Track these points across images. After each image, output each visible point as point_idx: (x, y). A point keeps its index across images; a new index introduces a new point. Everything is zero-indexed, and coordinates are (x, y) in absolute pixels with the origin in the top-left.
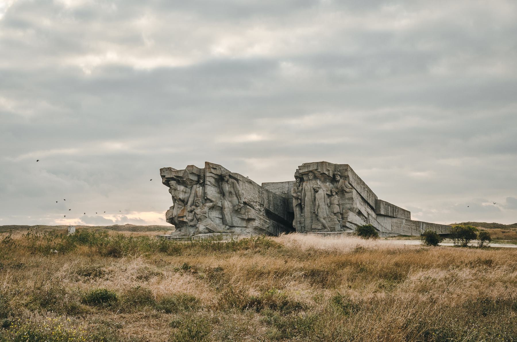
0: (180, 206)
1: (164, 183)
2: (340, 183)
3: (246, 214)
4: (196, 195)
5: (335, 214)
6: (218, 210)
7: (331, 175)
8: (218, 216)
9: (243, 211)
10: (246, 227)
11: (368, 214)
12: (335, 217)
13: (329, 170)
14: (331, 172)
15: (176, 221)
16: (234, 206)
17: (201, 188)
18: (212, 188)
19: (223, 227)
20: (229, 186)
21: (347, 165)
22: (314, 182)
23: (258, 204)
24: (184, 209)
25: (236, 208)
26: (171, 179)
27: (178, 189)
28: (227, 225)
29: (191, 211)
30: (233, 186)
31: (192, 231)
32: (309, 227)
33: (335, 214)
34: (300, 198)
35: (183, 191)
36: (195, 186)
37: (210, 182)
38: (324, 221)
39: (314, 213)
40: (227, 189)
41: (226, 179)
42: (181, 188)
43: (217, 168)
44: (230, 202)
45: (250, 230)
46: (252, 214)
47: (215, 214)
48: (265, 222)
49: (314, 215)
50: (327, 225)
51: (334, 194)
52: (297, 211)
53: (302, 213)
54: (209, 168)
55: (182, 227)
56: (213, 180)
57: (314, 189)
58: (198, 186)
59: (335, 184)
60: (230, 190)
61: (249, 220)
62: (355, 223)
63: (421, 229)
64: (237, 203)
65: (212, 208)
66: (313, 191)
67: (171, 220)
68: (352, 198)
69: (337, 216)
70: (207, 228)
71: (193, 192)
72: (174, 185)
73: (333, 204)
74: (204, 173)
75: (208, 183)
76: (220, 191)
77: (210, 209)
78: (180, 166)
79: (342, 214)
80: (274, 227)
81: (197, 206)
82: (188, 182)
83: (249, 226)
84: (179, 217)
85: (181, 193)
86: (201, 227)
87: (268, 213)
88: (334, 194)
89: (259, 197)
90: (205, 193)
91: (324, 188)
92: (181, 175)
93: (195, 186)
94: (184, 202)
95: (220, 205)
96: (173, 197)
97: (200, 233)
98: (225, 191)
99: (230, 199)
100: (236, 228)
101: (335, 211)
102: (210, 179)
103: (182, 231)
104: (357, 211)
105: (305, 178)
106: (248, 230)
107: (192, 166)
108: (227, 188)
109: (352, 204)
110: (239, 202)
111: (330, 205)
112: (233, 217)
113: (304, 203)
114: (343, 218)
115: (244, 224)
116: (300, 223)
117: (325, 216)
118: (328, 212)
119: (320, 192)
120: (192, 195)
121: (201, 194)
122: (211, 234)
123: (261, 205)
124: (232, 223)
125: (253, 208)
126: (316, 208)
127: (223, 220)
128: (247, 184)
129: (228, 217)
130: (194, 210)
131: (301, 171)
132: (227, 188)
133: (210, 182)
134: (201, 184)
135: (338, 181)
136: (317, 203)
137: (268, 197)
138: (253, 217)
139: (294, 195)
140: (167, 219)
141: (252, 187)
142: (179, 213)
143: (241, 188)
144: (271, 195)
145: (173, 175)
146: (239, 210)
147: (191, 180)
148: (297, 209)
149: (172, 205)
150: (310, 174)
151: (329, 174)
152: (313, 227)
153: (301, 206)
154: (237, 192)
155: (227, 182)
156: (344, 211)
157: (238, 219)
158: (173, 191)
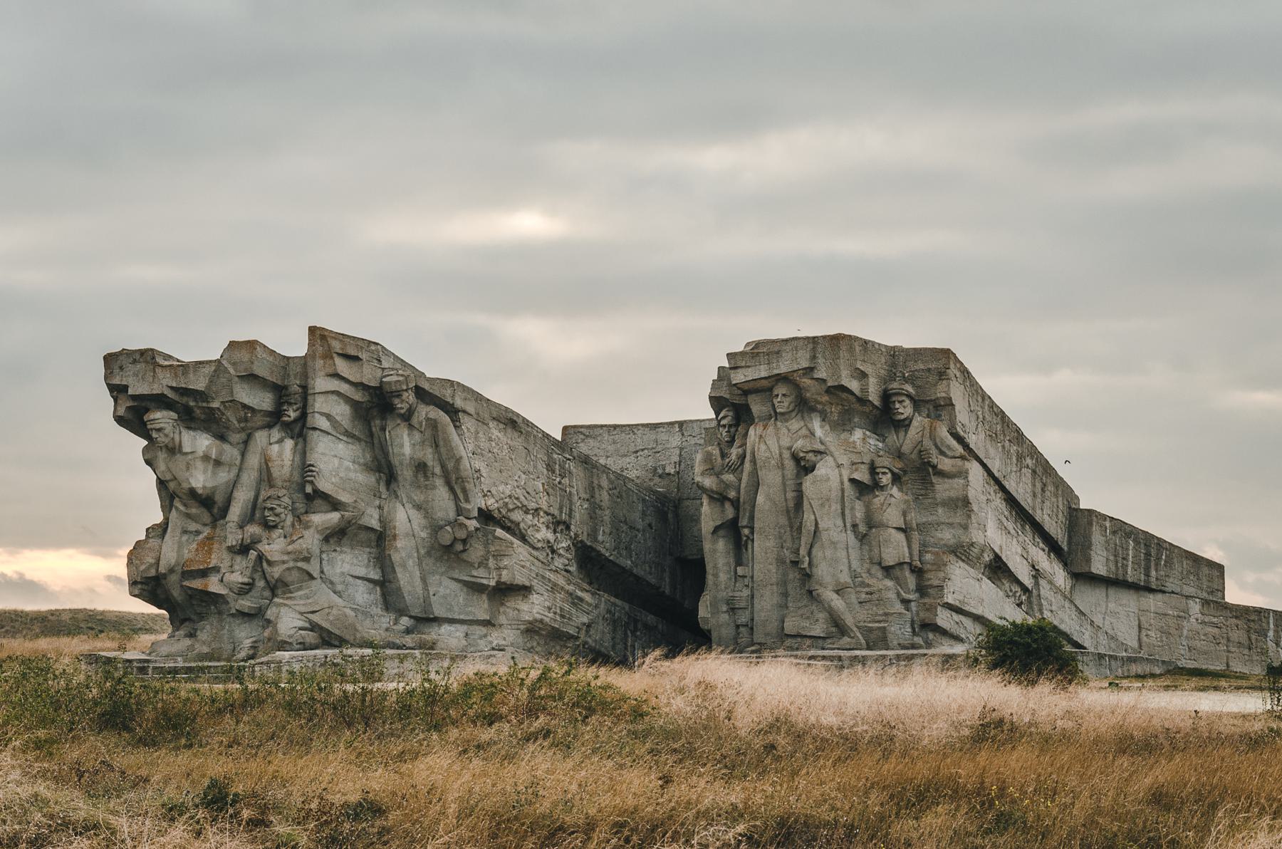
0: (193, 526)
1: (120, 420)
2: (912, 431)
3: (491, 563)
4: (266, 477)
5: (888, 570)
6: (362, 544)
7: (874, 397)
8: (362, 572)
9: (476, 551)
10: (488, 623)
11: (1037, 574)
12: (889, 583)
13: (863, 375)
14: (872, 381)
15: (176, 593)
16: (435, 529)
17: (289, 443)
18: (341, 446)
19: (386, 620)
20: (417, 436)
21: (947, 353)
22: (795, 424)
23: (545, 519)
24: (210, 538)
25: (446, 538)
26: (151, 398)
27: (186, 449)
28: (401, 612)
29: (243, 549)
30: (435, 437)
31: (245, 635)
32: (773, 627)
33: (888, 570)
34: (732, 494)
35: (206, 458)
36: (260, 437)
37: (328, 417)
38: (837, 603)
39: (795, 563)
40: (407, 450)
41: (402, 406)
42: (201, 442)
43: (364, 356)
44: (418, 507)
45: (507, 635)
46: (518, 563)
47: (350, 563)
48: (576, 601)
49: (793, 575)
50: (849, 621)
51: (886, 479)
52: (717, 553)
53: (739, 562)
54: (328, 355)
55: (202, 617)
56: (341, 411)
57: (796, 458)
58: (276, 434)
59: (892, 438)
60: (419, 455)
61: (505, 591)
62: (978, 611)
63: (1271, 644)
64: (452, 515)
65: (336, 536)
66: (789, 464)
67: (148, 585)
68: (966, 502)
69: (897, 580)
70: (314, 627)
71: (254, 460)
72: (168, 429)
74: (305, 375)
75: (323, 423)
76: (375, 458)
77: (326, 539)
78: (196, 344)
79: (918, 572)
80: (614, 623)
81: (268, 527)
82: (231, 416)
83: (502, 619)
84: (188, 574)
85: (199, 465)
86: (288, 621)
87: (589, 561)
88: (886, 479)
89: (550, 488)
90: (305, 468)
91: (843, 453)
92: (199, 383)
93: (260, 437)
94: (211, 506)
95: (375, 524)
96: (161, 484)
97: (283, 646)
98: (395, 461)
99: (418, 497)
100: (446, 628)
101: (890, 560)
102: (329, 407)
103: (203, 635)
104: (987, 557)
105: (757, 407)
106: (496, 637)
107: (252, 345)
108: (405, 445)
109: (965, 527)
110: (459, 511)
111: (867, 531)
112: (433, 579)
113: (752, 518)
114: (922, 590)
115: (481, 609)
116: (733, 610)
117: (845, 578)
118: (855, 564)
119: (824, 469)
120: (249, 478)
121: (286, 470)
122: (330, 652)
123: (559, 525)
124: (427, 603)
125: (523, 538)
126: (805, 541)
127: (386, 586)
128: (495, 431)
129: (408, 579)
130: (256, 541)
131: (739, 377)
132: (405, 445)
133: (328, 417)
134: (287, 427)
135: (904, 425)
136: (808, 518)
137: (592, 489)
138: (521, 580)
139: (708, 482)
140: (133, 583)
141: (518, 442)
142: (187, 555)
143: (468, 444)
144: (605, 483)
145: (163, 384)
146: (459, 547)
147: (245, 406)
148: (721, 545)
149: (158, 518)
150: (781, 390)
151: (864, 390)
152: (790, 626)
153: (736, 534)
154: (450, 465)
155: (407, 417)
156: (928, 557)
157: (455, 586)
158: (162, 456)
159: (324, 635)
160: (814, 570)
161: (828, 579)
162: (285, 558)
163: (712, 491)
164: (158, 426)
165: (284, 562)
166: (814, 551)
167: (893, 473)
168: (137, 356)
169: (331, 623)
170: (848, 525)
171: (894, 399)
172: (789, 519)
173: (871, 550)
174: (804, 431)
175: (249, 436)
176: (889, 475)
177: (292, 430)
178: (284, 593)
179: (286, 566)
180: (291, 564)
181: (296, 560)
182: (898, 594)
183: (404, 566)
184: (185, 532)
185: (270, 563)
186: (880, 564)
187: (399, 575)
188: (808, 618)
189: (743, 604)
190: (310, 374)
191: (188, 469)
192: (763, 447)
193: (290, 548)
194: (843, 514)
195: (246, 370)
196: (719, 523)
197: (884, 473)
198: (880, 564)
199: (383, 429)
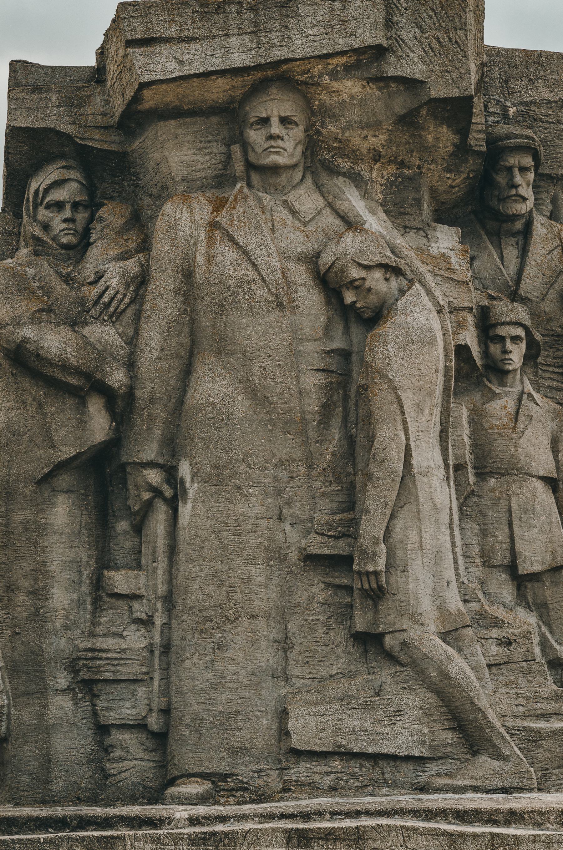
32: (259, 730)
33: (522, 581)
34: (117, 378)
38: (459, 665)
49: (314, 590)
51: (516, 354)
53: (104, 562)
66: (310, 301)
73: (513, 471)
105: (177, 153)
116: (88, 684)
117: (454, 602)
126: (376, 501)
148: (62, 513)
150: (276, 105)
152: (306, 728)
160: (397, 579)
161: (426, 605)
163: (65, 367)
166: (398, 526)
167: (532, 344)
170: (451, 463)
171: (513, 160)
172: (306, 442)
173: (484, 534)
174: (329, 220)
176: (523, 345)
182: (544, 645)
186: (512, 568)
188: (367, 706)
189: (130, 670)
192: (226, 254)
194: (443, 436)
196: (67, 452)
197: (515, 339)
198: (512, 568)
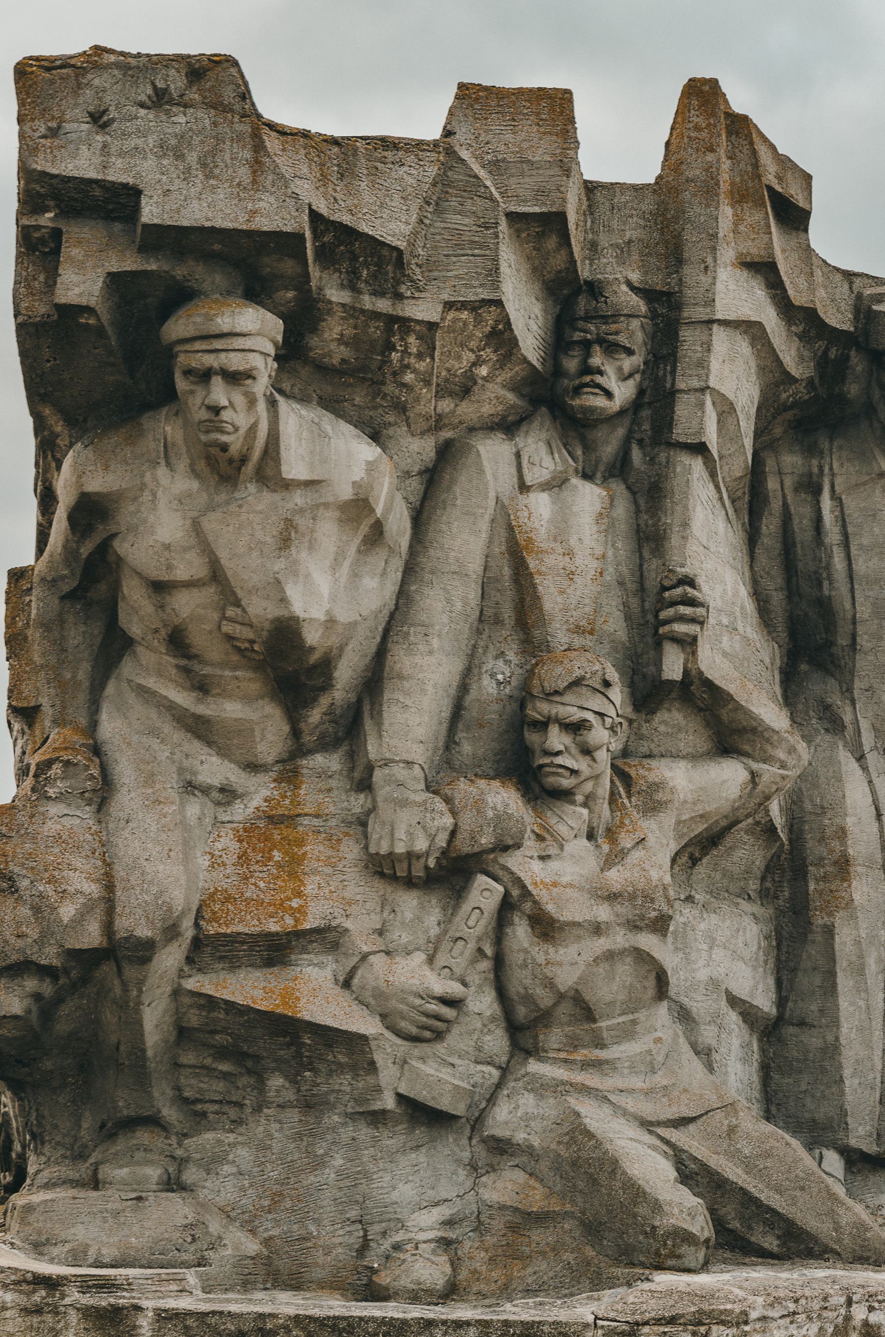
0: (214, 769)
24: (277, 819)
27: (295, 464)
29: (450, 873)
71: (465, 541)
84: (207, 950)
85: (328, 532)
120: (448, 604)
159: (730, 1211)
162: (603, 913)
164: (235, 362)
165: (597, 929)
168: (176, 82)
169: (749, 1167)
175: (446, 454)
177: (588, 447)
178: (574, 1044)
179: (602, 944)
180: (620, 939)
181: (634, 926)
183: (860, 970)
184: (191, 787)
185: (546, 927)
187: (844, 1003)
190: (691, 252)
191: (285, 542)
193: (616, 877)
195: (541, 193)
199: (811, 487)
